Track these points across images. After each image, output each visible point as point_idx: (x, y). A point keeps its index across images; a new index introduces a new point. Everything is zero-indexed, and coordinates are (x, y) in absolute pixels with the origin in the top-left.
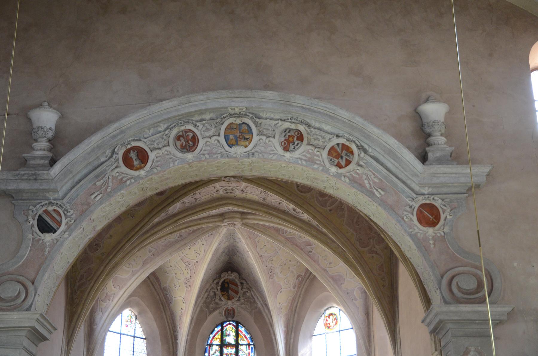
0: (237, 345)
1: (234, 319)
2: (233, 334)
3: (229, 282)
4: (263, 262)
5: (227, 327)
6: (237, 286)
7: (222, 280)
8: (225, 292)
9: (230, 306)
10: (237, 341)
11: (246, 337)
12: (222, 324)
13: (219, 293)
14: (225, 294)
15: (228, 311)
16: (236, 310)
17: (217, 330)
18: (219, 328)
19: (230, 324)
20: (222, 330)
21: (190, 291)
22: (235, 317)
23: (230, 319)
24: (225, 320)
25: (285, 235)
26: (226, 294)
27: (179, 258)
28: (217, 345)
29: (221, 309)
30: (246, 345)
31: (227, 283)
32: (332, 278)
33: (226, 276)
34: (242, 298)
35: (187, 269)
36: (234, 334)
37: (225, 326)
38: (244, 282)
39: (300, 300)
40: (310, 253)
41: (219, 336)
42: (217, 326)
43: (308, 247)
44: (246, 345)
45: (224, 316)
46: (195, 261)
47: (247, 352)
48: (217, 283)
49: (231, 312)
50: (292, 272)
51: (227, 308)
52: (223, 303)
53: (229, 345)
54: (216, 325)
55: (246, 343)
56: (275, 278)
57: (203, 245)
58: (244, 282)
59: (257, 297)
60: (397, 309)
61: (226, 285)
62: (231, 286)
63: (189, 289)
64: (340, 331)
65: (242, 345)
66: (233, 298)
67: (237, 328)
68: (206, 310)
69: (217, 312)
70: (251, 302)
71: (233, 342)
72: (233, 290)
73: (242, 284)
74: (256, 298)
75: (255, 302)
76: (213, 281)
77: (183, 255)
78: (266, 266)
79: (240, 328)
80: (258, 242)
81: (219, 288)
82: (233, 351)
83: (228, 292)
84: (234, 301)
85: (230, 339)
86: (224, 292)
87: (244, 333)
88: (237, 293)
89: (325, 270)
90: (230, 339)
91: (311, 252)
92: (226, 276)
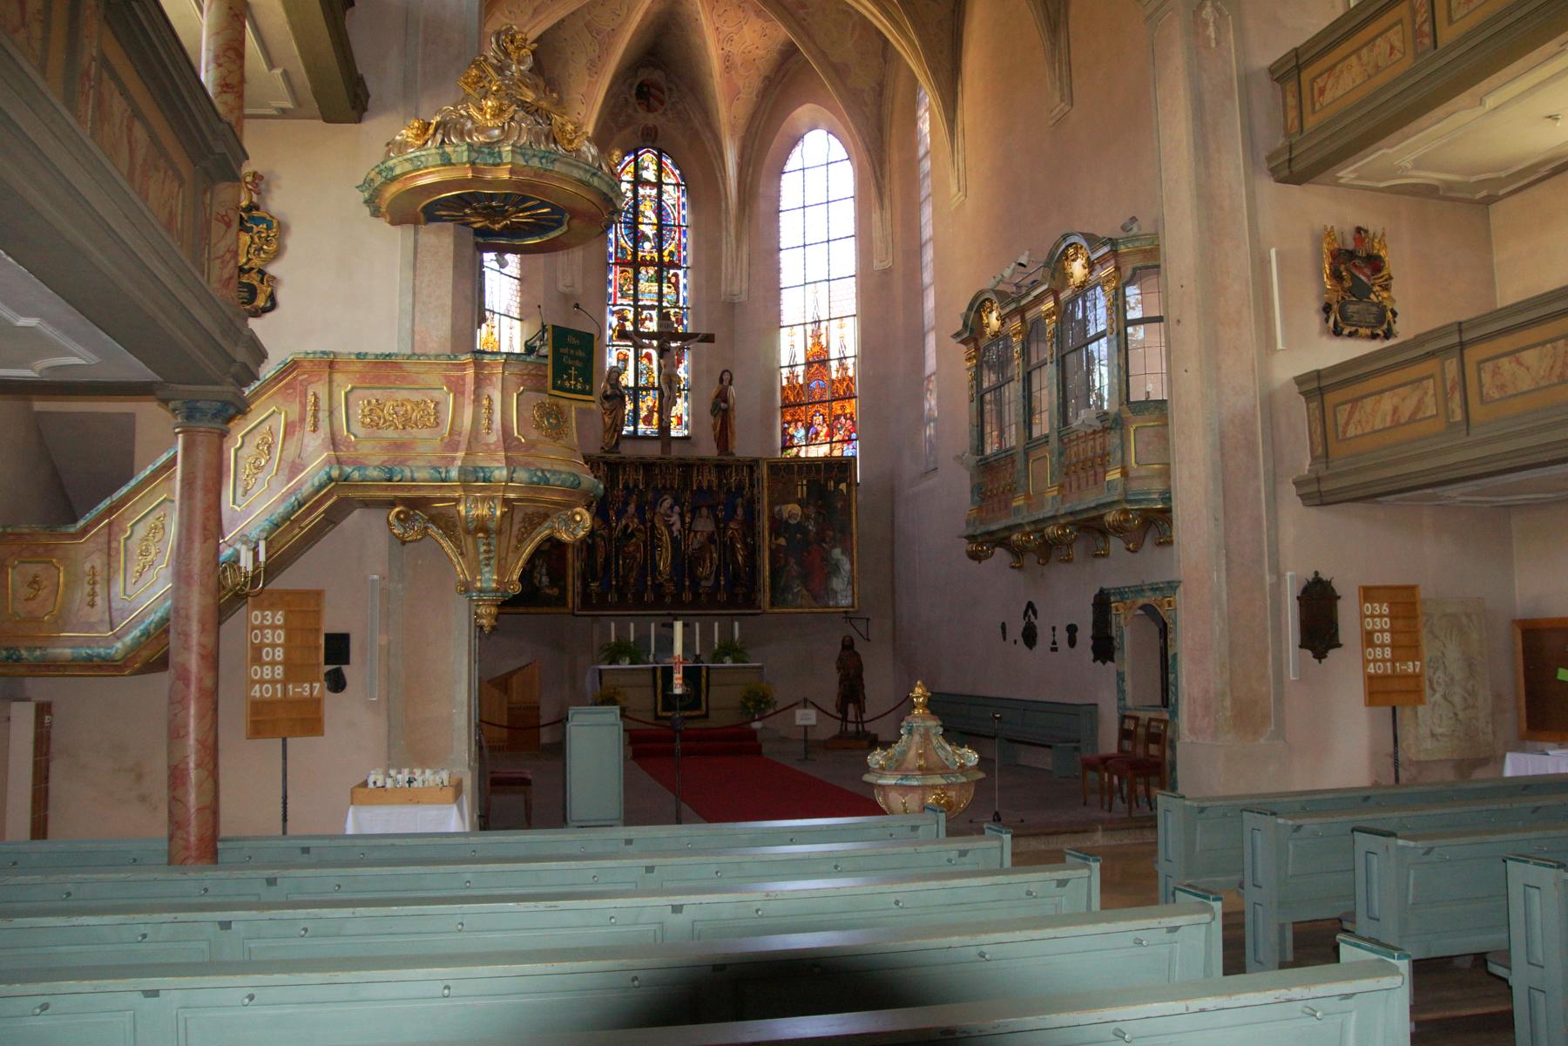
0: (659, 185)
1: (654, 145)
2: (653, 167)
4: (719, 40)
5: (644, 156)
6: (663, 92)
7: (638, 81)
10: (659, 177)
11: (673, 173)
12: (635, 152)
13: (633, 100)
17: (627, 159)
18: (632, 157)
19: (649, 152)
20: (636, 160)
21: (597, 81)
23: (649, 144)
24: (641, 144)
28: (628, 182)
30: (674, 185)
31: (648, 87)
32: (834, 66)
33: (644, 74)
36: (655, 168)
38: (674, 88)
39: (764, 118)
41: (631, 168)
42: (628, 154)
44: (674, 185)
46: (609, 29)
47: (676, 196)
48: (631, 85)
50: (758, 69)
53: (647, 183)
55: (674, 182)
56: (733, 73)
58: (674, 88)
60: (960, 88)
61: (645, 89)
62: (652, 90)
63: (593, 80)
64: (828, 164)
65: (667, 184)
66: (656, 110)
67: (659, 158)
69: (630, 129)
71: (653, 179)
72: (656, 98)
73: (670, 89)
74: (691, 114)
76: (624, 82)
77: (588, 17)
79: (664, 159)
81: (634, 92)
82: (654, 192)
83: (648, 100)
84: (655, 113)
85: (649, 175)
87: (670, 166)
88: (662, 103)
90: (649, 175)
91: (805, 20)
92: (644, 74)
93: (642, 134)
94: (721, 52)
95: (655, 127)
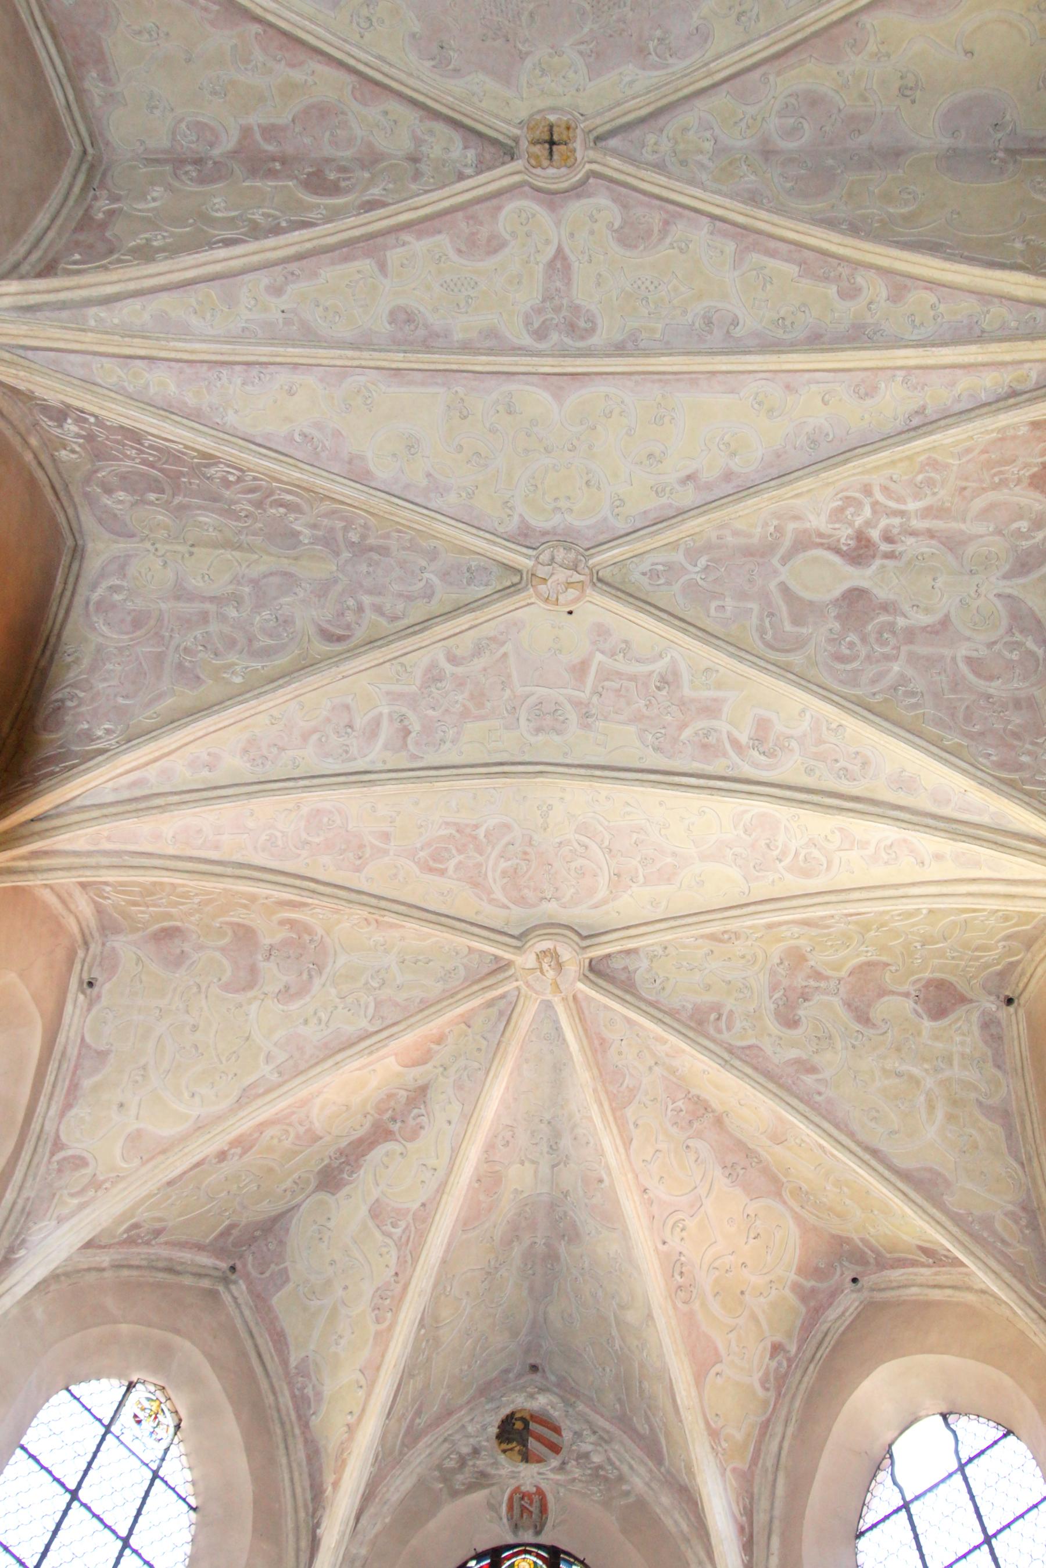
1: (542, 1539)
3: (528, 1418)
8: (514, 1444)
9: (528, 1483)
14: (511, 1449)
15: (522, 1498)
16: (550, 1498)
22: (546, 1529)
24: (510, 1539)
25: (725, 1036)
26: (518, 1448)
27: (364, 1210)
29: (494, 1488)
34: (574, 1463)
35: (384, 1250)
37: (508, 1558)
39: (790, 1430)
40: (817, 1098)
43: (809, 1079)
45: (505, 1520)
49: (531, 1504)
51: (517, 1490)
52: (503, 1472)
54: (473, 1553)
57: (449, 1122)
59: (631, 1467)
68: (441, 1486)
69: (479, 1496)
70: (606, 1479)
72: (540, 1439)
75: (621, 1479)
77: (375, 1193)
78: (664, 1243)
80: (636, 1125)
86: (509, 1441)
89: (874, 1153)
91: (819, 1094)
92: (519, 1402)
93: (510, 1508)
94: (660, 1246)
95: (540, 1492)
